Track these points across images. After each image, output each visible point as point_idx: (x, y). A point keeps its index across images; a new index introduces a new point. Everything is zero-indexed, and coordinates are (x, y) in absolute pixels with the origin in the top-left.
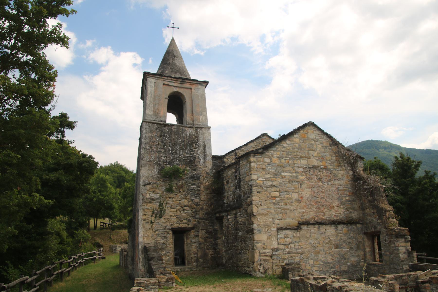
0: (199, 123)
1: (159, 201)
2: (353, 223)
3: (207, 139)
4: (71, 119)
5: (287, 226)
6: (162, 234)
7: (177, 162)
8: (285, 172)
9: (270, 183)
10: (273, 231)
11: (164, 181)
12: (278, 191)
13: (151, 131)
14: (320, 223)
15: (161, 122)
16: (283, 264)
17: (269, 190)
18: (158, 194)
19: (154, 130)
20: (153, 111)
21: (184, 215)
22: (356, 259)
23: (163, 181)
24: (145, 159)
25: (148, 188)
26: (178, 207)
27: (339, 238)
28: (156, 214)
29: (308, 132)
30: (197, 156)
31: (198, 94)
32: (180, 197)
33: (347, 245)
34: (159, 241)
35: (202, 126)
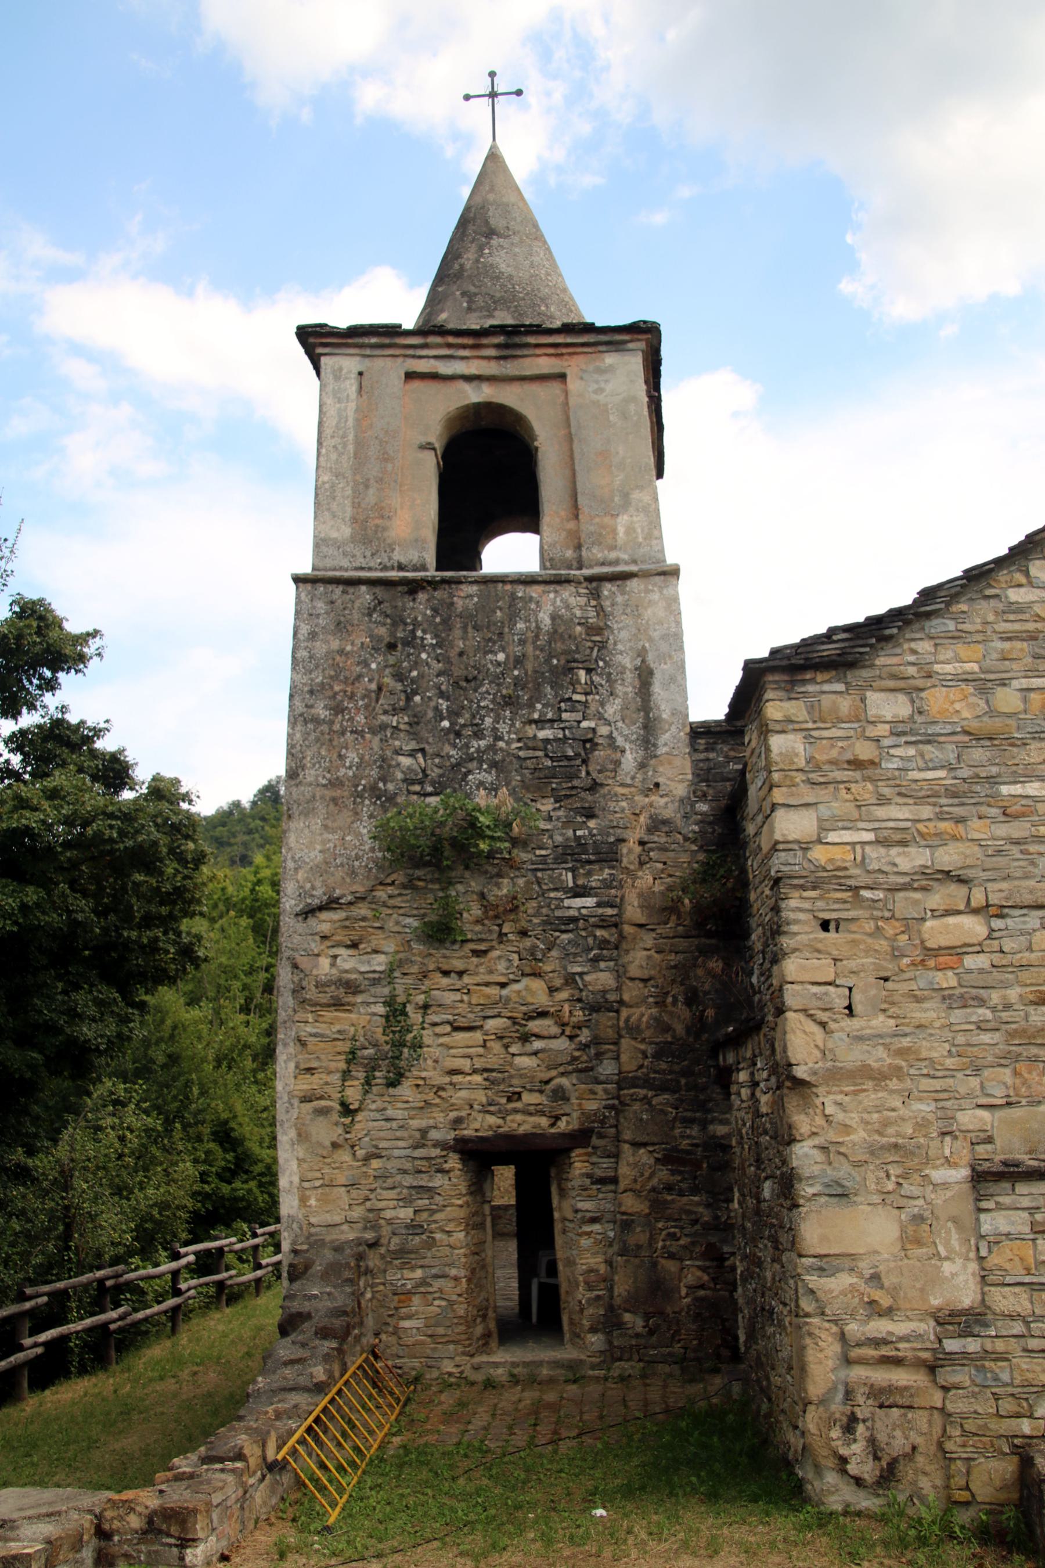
0: (613, 555)
1: (386, 991)
3: (656, 635)
6: (405, 1172)
7: (483, 776)
8: (1030, 776)
9: (911, 859)
10: (945, 1186)
11: (409, 885)
12: (975, 911)
13: (341, 627)
15: (394, 574)
18: (382, 958)
19: (356, 616)
20: (354, 520)
21: (525, 1062)
23: (404, 886)
25: (325, 928)
26: (491, 1024)
30: (604, 730)
31: (601, 398)
32: (501, 966)
34: (388, 1214)
35: (634, 568)
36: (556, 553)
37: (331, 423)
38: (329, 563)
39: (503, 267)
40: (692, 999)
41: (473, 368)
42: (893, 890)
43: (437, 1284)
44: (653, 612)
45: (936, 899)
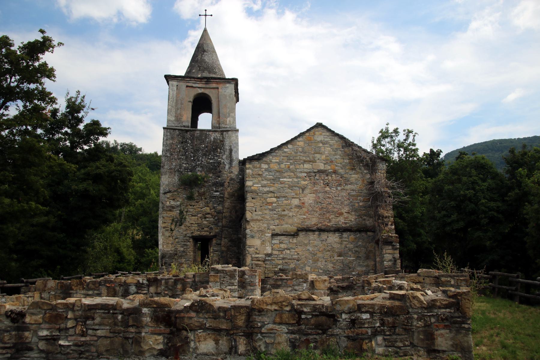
2: (363, 231)
4: (104, 125)
5: (284, 232)
7: (199, 169)
8: (285, 177)
11: (184, 189)
13: (172, 138)
14: (321, 230)
15: (183, 128)
16: (276, 269)
17: (265, 196)
20: (175, 116)
21: (205, 222)
22: (364, 269)
24: (166, 167)
25: (168, 196)
27: (343, 246)
28: (177, 222)
30: (222, 161)
32: (201, 205)
33: (353, 253)
35: (230, 129)
36: (215, 125)
37: (171, 96)
38: (170, 125)
40: (236, 212)
41: (200, 85)
42: (263, 194)
43: (188, 262)
44: (233, 138)
45: (269, 195)
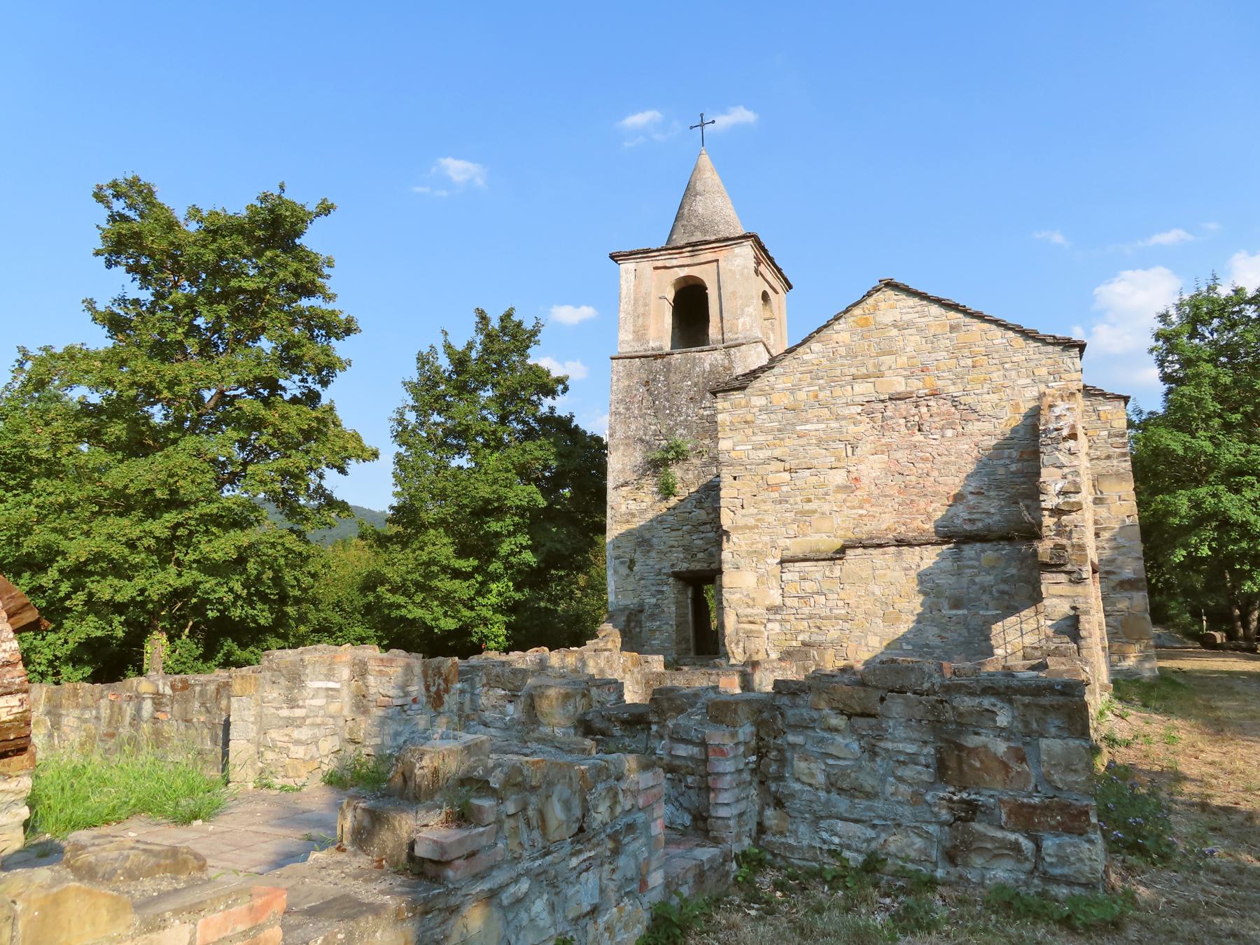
8: (807, 422)
14: (900, 543)
16: (794, 643)
17: (761, 470)
27: (965, 581)
29: (876, 308)
33: (993, 598)
39: (700, 210)
43: (665, 627)
